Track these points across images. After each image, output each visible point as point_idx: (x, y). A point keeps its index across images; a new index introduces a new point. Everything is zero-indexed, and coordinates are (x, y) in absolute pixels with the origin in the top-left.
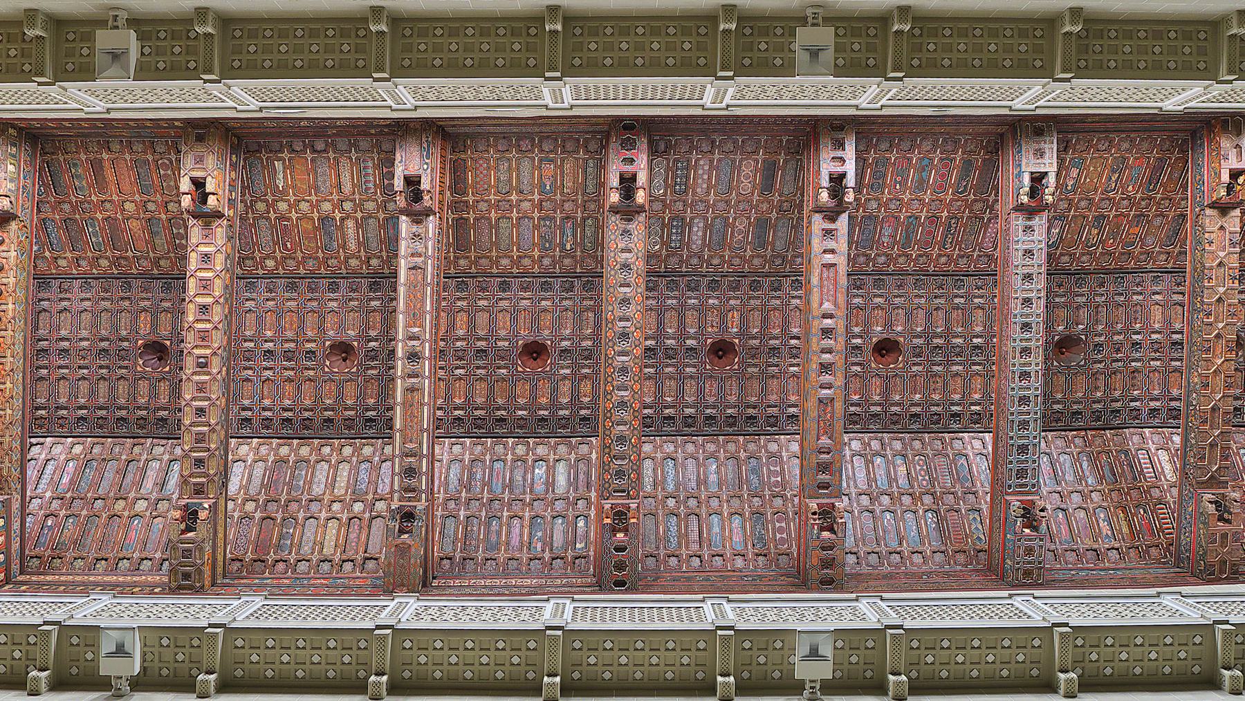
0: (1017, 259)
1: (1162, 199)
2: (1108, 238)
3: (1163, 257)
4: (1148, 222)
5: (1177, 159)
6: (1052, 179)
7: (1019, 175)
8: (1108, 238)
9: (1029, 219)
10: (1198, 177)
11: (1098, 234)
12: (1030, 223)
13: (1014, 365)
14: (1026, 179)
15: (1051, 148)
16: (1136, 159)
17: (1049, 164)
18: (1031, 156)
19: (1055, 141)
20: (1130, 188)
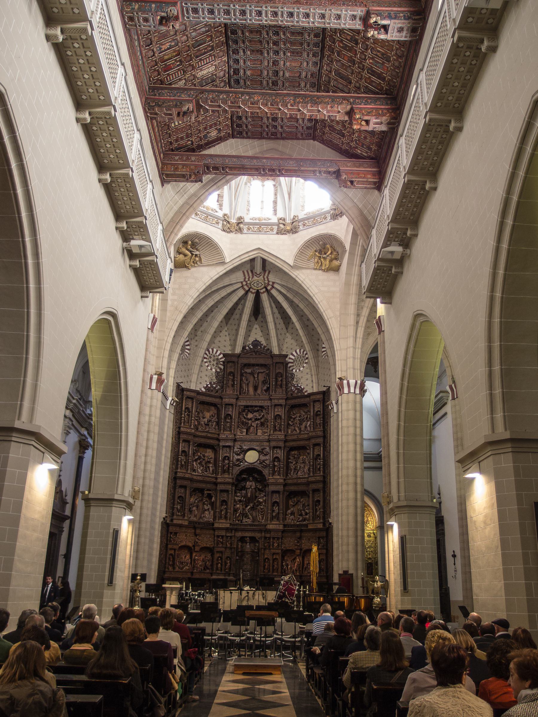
0: (335, 11)
1: (362, 75)
2: (343, 44)
3: (329, 69)
4: (350, 66)
5: (383, 87)
6: (382, 37)
7: (390, 17)
8: (343, 44)
9: (360, 19)
10: (369, 101)
11: (347, 39)
12: (358, 19)
13: (266, 7)
14: (385, 22)
15: (403, 37)
16: (388, 67)
17: (393, 35)
18: (400, 25)
19: (406, 39)
20: (371, 61)
